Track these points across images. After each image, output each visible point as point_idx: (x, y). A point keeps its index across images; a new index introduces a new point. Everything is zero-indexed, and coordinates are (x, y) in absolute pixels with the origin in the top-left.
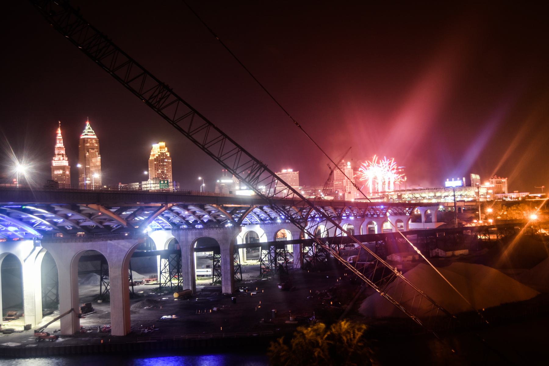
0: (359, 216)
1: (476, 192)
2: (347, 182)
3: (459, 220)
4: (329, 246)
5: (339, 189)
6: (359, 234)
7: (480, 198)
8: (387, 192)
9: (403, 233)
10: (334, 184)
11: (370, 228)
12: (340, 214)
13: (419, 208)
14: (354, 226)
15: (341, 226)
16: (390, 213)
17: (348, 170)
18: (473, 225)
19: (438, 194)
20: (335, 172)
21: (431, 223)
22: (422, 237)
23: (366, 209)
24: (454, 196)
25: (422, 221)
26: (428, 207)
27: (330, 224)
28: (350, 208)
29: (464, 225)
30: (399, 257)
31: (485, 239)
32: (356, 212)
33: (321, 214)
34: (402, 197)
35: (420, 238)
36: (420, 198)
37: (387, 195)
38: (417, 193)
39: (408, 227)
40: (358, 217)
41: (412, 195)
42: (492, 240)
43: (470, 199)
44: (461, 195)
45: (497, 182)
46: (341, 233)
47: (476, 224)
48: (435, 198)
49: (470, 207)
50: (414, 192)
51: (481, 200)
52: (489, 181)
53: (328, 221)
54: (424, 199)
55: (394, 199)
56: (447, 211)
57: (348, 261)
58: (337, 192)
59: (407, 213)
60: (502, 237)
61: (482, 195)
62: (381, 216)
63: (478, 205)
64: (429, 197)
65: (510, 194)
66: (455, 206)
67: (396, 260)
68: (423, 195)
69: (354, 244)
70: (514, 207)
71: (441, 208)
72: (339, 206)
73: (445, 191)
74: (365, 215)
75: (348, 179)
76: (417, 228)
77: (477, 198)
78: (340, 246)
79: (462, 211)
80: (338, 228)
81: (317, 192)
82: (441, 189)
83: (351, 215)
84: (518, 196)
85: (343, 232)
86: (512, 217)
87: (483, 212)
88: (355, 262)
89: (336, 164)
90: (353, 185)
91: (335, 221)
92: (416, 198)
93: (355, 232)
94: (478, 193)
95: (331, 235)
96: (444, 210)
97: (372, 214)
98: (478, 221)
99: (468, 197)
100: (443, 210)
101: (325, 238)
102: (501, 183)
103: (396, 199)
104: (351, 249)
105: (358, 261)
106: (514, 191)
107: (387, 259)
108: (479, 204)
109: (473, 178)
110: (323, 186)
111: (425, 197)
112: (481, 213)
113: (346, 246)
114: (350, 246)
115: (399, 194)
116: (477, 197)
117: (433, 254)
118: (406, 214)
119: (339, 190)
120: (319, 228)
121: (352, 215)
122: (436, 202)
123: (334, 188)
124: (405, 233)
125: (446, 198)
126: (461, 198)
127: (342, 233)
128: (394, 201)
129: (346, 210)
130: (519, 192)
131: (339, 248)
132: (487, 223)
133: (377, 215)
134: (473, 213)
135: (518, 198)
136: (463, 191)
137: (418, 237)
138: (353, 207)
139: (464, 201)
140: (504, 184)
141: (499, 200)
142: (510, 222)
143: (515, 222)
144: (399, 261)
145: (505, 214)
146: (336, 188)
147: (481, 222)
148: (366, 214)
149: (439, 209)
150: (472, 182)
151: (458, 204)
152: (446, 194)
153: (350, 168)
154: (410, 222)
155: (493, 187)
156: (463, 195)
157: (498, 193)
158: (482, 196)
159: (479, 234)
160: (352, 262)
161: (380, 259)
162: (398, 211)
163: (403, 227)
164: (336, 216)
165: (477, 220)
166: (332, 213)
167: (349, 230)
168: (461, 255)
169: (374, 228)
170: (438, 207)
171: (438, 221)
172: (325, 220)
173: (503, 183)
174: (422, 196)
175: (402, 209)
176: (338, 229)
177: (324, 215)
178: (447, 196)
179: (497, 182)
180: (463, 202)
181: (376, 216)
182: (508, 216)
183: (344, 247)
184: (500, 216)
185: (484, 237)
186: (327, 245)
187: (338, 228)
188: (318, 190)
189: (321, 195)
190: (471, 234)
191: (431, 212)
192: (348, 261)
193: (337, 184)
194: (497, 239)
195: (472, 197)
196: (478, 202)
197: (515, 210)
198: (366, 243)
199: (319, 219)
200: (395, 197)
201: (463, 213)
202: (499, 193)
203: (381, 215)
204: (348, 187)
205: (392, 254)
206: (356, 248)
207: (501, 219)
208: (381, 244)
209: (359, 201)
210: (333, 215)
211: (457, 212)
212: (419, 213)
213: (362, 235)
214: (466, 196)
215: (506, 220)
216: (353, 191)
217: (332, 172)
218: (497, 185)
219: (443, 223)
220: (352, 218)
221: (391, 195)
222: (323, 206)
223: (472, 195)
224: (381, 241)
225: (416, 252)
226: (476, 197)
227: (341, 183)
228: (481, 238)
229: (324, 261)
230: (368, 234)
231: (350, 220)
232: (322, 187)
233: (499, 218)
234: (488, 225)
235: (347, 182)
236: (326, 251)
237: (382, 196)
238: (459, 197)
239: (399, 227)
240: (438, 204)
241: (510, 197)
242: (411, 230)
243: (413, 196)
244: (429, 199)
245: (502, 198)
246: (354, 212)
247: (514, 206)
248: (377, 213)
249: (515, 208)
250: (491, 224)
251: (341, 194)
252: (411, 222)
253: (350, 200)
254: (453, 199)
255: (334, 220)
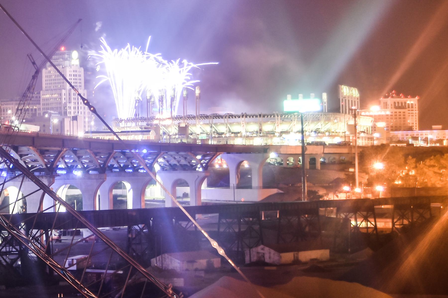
0: (94, 170)
1: (349, 126)
2: (69, 94)
3: (311, 185)
4: (27, 231)
5: (52, 109)
6: (92, 210)
7: (358, 138)
8: (157, 119)
9: (191, 210)
10: (41, 100)
11: (115, 197)
12: (52, 163)
13: (225, 155)
14: (82, 191)
15: (54, 191)
16: (160, 166)
17: (72, 70)
18: (342, 197)
19: (267, 127)
20: (44, 71)
21: (249, 190)
22: (231, 220)
23: (110, 154)
24: (302, 132)
25: (231, 185)
26: (244, 155)
27: (30, 185)
28: (75, 152)
29: (321, 196)
30: (179, 261)
31: (367, 228)
32: (87, 161)
33: (11, 162)
34: (189, 132)
35: (225, 221)
36: (228, 135)
37: (156, 125)
38: (222, 124)
39: (200, 196)
40: (90, 172)
41: (211, 127)
42: (382, 230)
43: (337, 140)
44: (317, 131)
45: (397, 105)
46: (53, 205)
47: (348, 194)
48: (261, 136)
49: (337, 157)
50: (215, 121)
51: (361, 142)
52: (379, 103)
53: (25, 178)
54: (237, 137)
55: (170, 134)
56: (285, 165)
57: (67, 266)
58: (47, 116)
59: (199, 166)
60: (402, 224)
61: (364, 132)
62: (142, 171)
63: (354, 154)
64: (248, 134)
65: (424, 132)
66: (303, 155)
67: (171, 267)
68: (235, 128)
69: (81, 230)
70: (431, 160)
71: (272, 157)
72: (50, 147)
73: (283, 121)
74: (107, 169)
75: (73, 87)
76: (218, 199)
77: (351, 138)
78: (50, 232)
79: (318, 166)
80: (46, 195)
81: (4, 114)
82: (274, 116)
83: (77, 166)
84: (441, 138)
85: (57, 203)
86: (426, 182)
87: (364, 170)
88: (83, 270)
89: (47, 54)
90: (81, 101)
91: (40, 179)
92: (218, 133)
93: (83, 204)
94: (353, 128)
95: (32, 209)
96: (278, 162)
97: (122, 165)
98: (352, 188)
99: (332, 136)
100: (278, 163)
101: (18, 214)
102: (406, 108)
103: (176, 134)
104: (74, 241)
105: (88, 268)
106: (434, 127)
107: (152, 265)
108: (356, 152)
109: (345, 94)
110: (18, 102)
111: (239, 133)
112: (359, 172)
113: (65, 234)
114: (72, 234)
115: (183, 125)
116: (353, 137)
117: (252, 256)
118: (197, 169)
119: (52, 112)
120: (5, 193)
121: (79, 166)
122: (263, 144)
123: (41, 107)
124: (193, 210)
125: (284, 135)
126: (317, 136)
127: (54, 206)
128: (170, 138)
129: (66, 156)
130: (443, 129)
131: (47, 237)
132: (373, 193)
133: (133, 168)
134: (343, 170)
135: (440, 141)
136: (322, 123)
137: (220, 219)
138: (81, 149)
139: (323, 144)
140: (410, 109)
141: (398, 145)
142: (423, 193)
143: (432, 193)
144: (178, 270)
145: (412, 176)
146: (45, 107)
147: (358, 190)
148: (108, 166)
149: (268, 161)
150: (341, 104)
151: (310, 150)
152: (284, 127)
153: (77, 65)
154: (204, 186)
155: (387, 115)
156: (322, 130)
157: (396, 128)
158: (362, 135)
159: (354, 216)
160: (74, 268)
161: (136, 265)
162: (179, 162)
163: (189, 195)
164: (44, 167)
165: (349, 185)
166: (35, 161)
167: (71, 198)
168: (312, 260)
169: (126, 196)
170: (265, 154)
171: (266, 186)
172: (18, 176)
173: (409, 107)
174: (232, 131)
175: (188, 157)
176: (46, 195)
177: (17, 166)
178: (287, 132)
179: (397, 105)
180: (322, 147)
181: (131, 171)
182: (418, 178)
183: (60, 236)
184: (402, 178)
185: (364, 225)
186: (22, 231)
187: (46, 194)
188: (7, 111)
189: (12, 122)
190: (337, 216)
191: (250, 165)
192: (67, 266)
193: (47, 99)
194: (392, 228)
195: (341, 137)
196: (354, 147)
197: (434, 166)
198: (107, 228)
199: (7, 173)
200: (174, 130)
201: (322, 168)
202: (400, 130)
203: (141, 169)
204: (72, 105)
205: (163, 256)
206: (85, 239)
207: (403, 185)
208: (139, 233)
209: (95, 136)
210: (37, 164)
211: (308, 166)
212: (225, 166)
213: (100, 211)
214: (327, 134)
215: (413, 189)
216: (82, 115)
217: (38, 72)
218: (396, 112)
219: (275, 191)
220: (78, 174)
221: (164, 126)
222: (16, 145)
223: (341, 131)
224: (140, 225)
225: (215, 251)
226: (349, 137)
227: (56, 96)
228: (357, 225)
229: (14, 265)
230: (112, 208)
231: (74, 178)
232: (16, 104)
233: (398, 182)
234: (373, 198)
235: (69, 94)
236: (20, 244)
237: (145, 128)
238: (313, 134)
239: (181, 195)
240: (265, 149)
241: (424, 137)
242: (206, 203)
243: (213, 130)
244: (247, 137)
245: (405, 139)
246: (84, 161)
247: (432, 157)
248: (132, 163)
249: (432, 163)
250: (381, 196)
251: (55, 121)
252: (206, 186)
253: (75, 134)
254: (301, 139)
255: (38, 176)
